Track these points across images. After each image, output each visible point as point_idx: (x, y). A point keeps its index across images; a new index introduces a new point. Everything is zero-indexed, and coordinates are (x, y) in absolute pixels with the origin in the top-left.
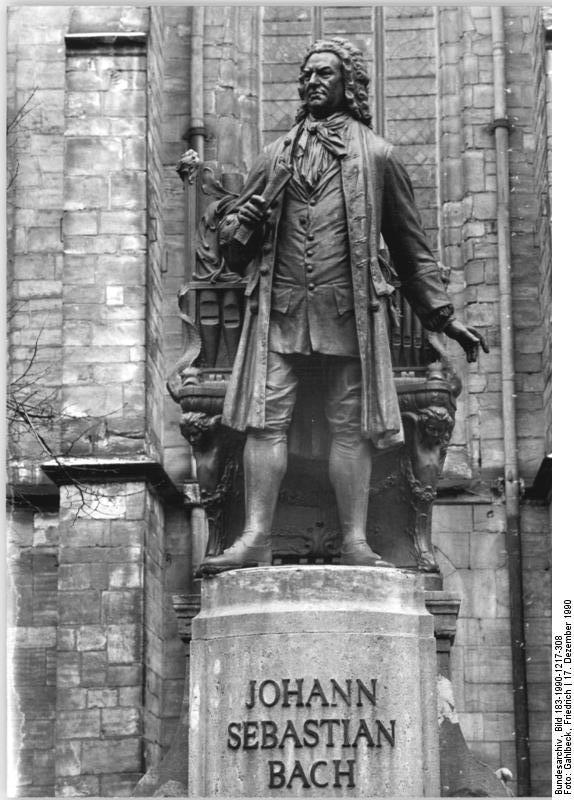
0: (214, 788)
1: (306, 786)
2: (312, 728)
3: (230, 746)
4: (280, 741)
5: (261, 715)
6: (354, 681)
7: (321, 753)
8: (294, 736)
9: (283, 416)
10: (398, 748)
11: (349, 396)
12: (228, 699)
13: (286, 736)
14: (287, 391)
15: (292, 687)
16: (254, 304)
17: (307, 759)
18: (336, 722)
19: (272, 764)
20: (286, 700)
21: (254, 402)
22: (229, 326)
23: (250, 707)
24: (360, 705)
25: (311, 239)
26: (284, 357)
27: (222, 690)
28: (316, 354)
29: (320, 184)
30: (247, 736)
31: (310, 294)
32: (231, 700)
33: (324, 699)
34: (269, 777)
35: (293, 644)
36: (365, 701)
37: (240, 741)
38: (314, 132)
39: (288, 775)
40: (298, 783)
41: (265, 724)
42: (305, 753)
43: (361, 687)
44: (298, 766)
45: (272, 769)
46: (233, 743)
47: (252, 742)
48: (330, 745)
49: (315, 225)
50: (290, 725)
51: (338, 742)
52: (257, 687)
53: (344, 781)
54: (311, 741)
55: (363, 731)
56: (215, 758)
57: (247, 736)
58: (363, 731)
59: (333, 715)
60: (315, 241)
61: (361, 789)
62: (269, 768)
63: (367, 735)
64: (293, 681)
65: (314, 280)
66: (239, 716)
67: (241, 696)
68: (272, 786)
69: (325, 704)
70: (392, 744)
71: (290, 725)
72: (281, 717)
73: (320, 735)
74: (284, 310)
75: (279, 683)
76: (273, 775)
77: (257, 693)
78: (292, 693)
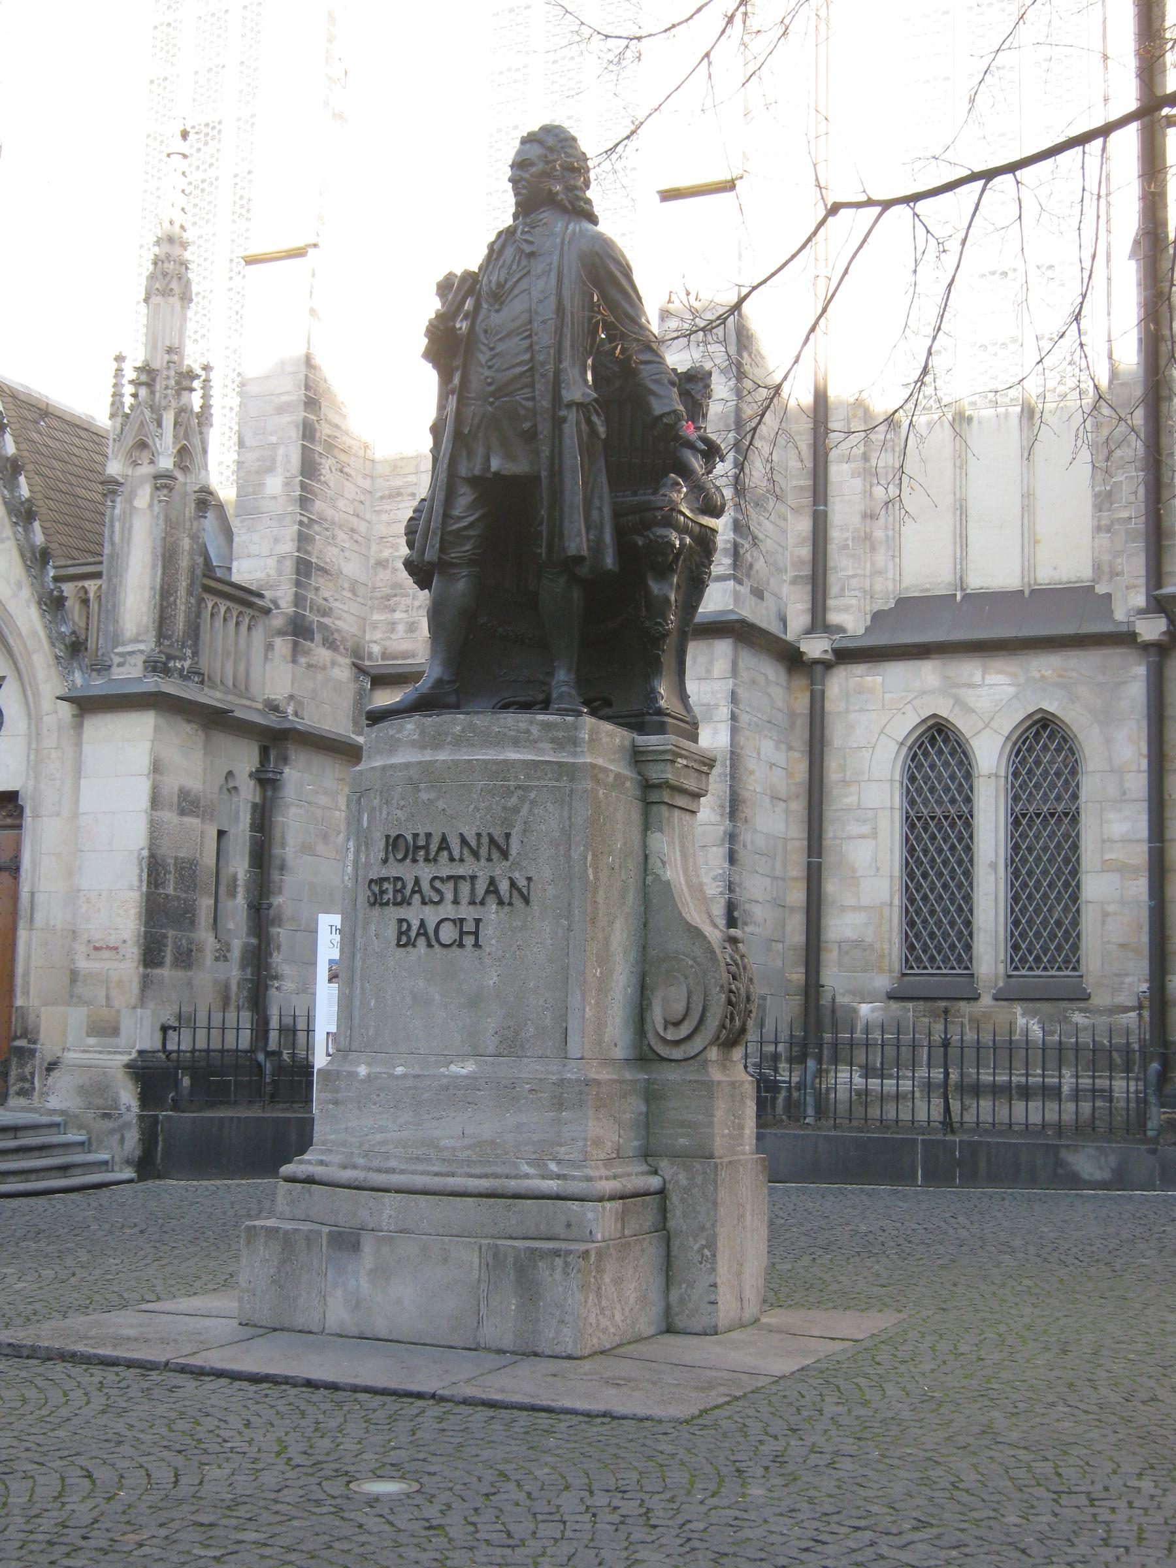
1: (430, 945)
2: (438, 884)
5: (393, 870)
6: (484, 834)
7: (447, 910)
8: (420, 891)
9: (468, 547)
10: (535, 906)
13: (413, 892)
14: (472, 518)
15: (421, 843)
17: (431, 916)
18: (462, 877)
20: (415, 853)
23: (385, 861)
24: (489, 860)
25: (492, 349)
27: (367, 845)
29: (507, 286)
30: (382, 892)
31: (490, 409)
33: (451, 854)
35: (424, 796)
36: (495, 855)
39: (413, 934)
40: (422, 941)
43: (492, 841)
44: (422, 924)
45: (400, 927)
47: (386, 897)
48: (456, 902)
49: (496, 334)
50: (417, 881)
53: (469, 941)
55: (492, 887)
56: (360, 915)
58: (492, 887)
59: (460, 870)
60: (497, 351)
61: (488, 950)
63: (496, 892)
65: (492, 394)
66: (377, 872)
68: (398, 945)
69: (452, 859)
70: (527, 901)
71: (417, 881)
72: (407, 872)
73: (443, 890)
75: (410, 838)
76: (400, 933)
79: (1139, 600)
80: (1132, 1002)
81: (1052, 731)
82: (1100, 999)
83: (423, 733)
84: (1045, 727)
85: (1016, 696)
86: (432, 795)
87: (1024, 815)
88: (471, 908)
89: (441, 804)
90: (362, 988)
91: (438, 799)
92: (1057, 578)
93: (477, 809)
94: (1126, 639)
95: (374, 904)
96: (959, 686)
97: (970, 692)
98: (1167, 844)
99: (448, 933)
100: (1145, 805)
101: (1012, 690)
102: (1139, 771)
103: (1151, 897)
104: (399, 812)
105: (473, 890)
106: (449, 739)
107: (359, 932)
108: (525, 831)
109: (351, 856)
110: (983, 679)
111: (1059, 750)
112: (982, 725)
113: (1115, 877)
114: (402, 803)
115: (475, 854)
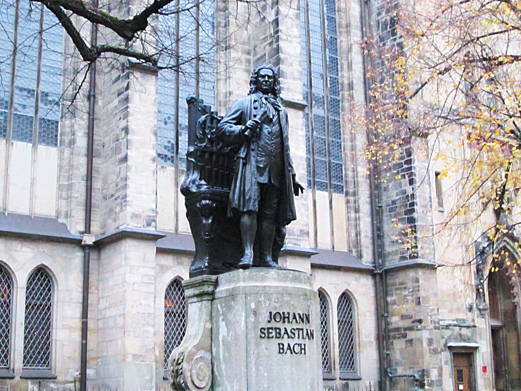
0: (252, 353)
1: (292, 353)
2: (293, 331)
3: (261, 337)
4: (282, 336)
5: (273, 324)
7: (296, 341)
8: (287, 333)
11: (275, 204)
12: (259, 318)
16: (244, 161)
19: (279, 344)
21: (252, 201)
22: (207, 167)
23: (269, 322)
26: (259, 184)
28: (273, 185)
32: (260, 319)
34: (278, 349)
35: (286, 299)
37: (265, 333)
38: (266, 99)
39: (285, 348)
40: (289, 351)
41: (276, 329)
42: (290, 340)
44: (289, 345)
46: (263, 336)
47: (271, 335)
48: (299, 338)
49: (274, 135)
51: (301, 337)
52: (273, 314)
53: (303, 351)
54: (293, 336)
56: (253, 342)
57: (269, 333)
59: (299, 327)
62: (278, 346)
64: (286, 313)
66: (265, 324)
67: (265, 317)
68: (280, 353)
69: (297, 322)
70: (313, 338)
74: (262, 166)
76: (280, 348)
77: (272, 317)
78: (286, 317)
79: (82, 228)
80: (72, 379)
81: (42, 273)
82: (61, 378)
83: (278, 275)
84: (39, 271)
85: (33, 258)
86: (289, 299)
87: (30, 305)
88: (303, 340)
89: (292, 302)
90: (257, 369)
91: (291, 300)
92: (42, 213)
93: (302, 305)
94: (77, 243)
95: (264, 338)
96: (11, 250)
97: (16, 253)
98: (88, 320)
99: (297, 349)
100: (81, 305)
101: (32, 255)
102: (77, 292)
103: (82, 340)
104: (276, 304)
105: (303, 334)
106: (289, 279)
107: (252, 348)
108: (312, 314)
109: (243, 318)
110: (21, 249)
111: (44, 280)
112: (20, 267)
113: (68, 331)
114: (277, 301)
115: (303, 321)
